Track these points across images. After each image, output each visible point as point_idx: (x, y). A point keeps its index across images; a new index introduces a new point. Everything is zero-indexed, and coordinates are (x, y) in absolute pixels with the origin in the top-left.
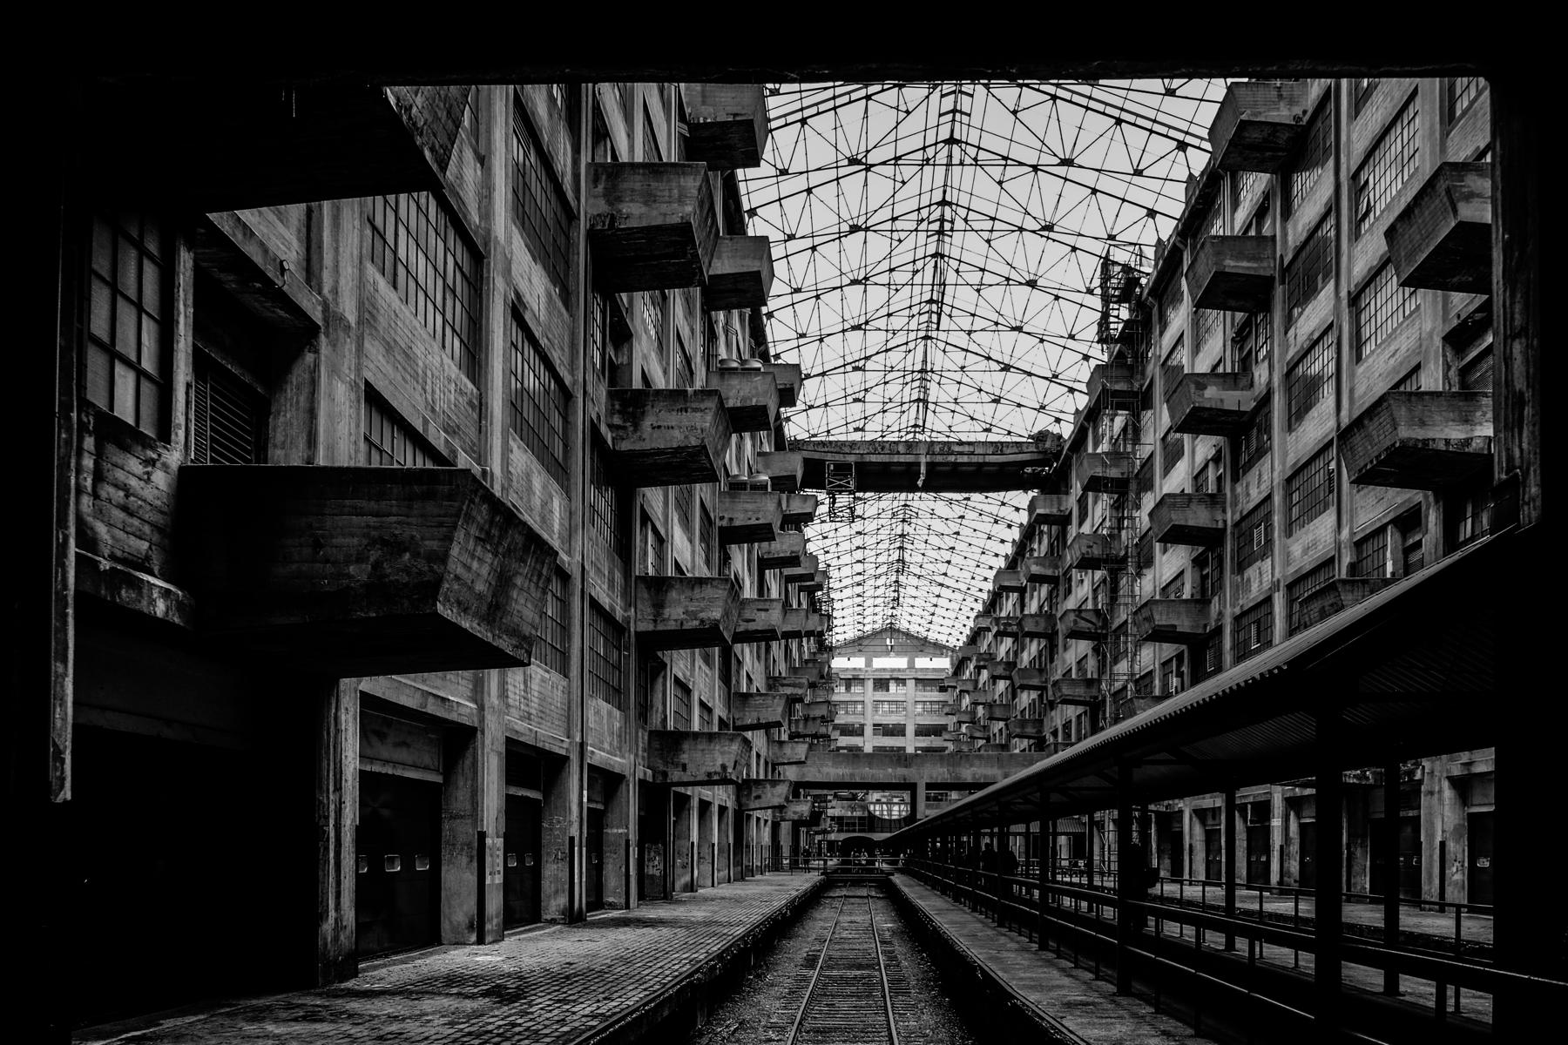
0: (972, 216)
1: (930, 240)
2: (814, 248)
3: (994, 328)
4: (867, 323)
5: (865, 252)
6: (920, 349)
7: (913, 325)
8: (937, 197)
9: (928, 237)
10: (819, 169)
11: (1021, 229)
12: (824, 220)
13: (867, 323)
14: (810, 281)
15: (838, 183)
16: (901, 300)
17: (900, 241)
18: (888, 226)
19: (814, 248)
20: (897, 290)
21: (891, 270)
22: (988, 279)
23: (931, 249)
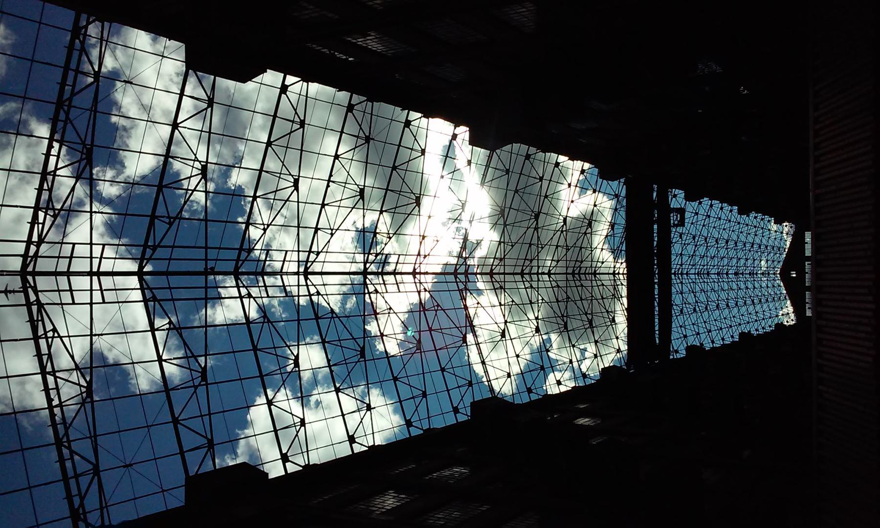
1: (541, 279)
4: (586, 314)
7: (589, 283)
9: (469, 281)
10: (507, 352)
15: (481, 343)
17: (543, 299)
20: (569, 298)
23: (546, 277)
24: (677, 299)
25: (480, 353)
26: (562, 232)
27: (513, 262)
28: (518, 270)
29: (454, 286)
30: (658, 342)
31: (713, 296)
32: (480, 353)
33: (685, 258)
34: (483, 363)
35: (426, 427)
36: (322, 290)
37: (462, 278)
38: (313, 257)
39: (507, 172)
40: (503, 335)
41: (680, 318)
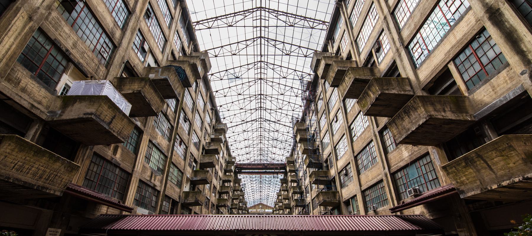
6: (260, 156)
8: (260, 117)
16: (255, 149)
22: (270, 139)
24: (254, 176)
25: (239, 125)
27: (264, 133)
28: (262, 135)
29: (257, 118)
30: (242, 171)
31: (255, 185)
32: (239, 125)
33: (265, 178)
34: (237, 125)
35: (220, 111)
36: (257, 83)
37: (260, 120)
38: (265, 81)
39: (288, 132)
40: (244, 131)
41: (249, 177)
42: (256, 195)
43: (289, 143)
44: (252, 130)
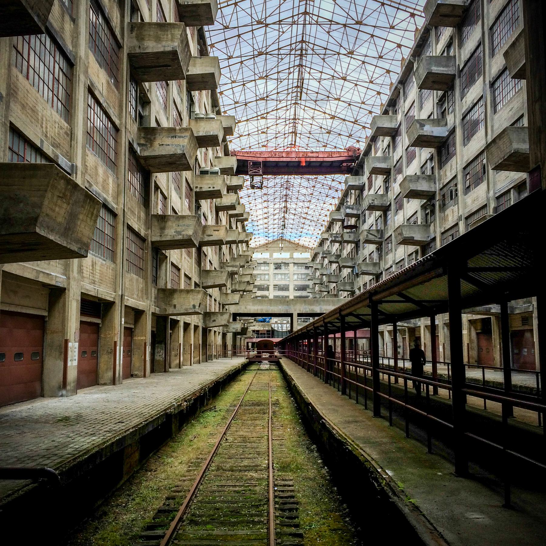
0: (316, 47)
1: (296, 59)
2: (242, 62)
3: (327, 99)
4: (267, 97)
5: (266, 64)
6: (293, 110)
7: (289, 98)
9: (295, 57)
11: (339, 54)
12: (247, 49)
13: (267, 97)
14: (240, 77)
17: (282, 59)
18: (276, 52)
19: (242, 62)
20: (281, 82)
21: (278, 72)
22: (324, 76)
23: (297, 63)
26: (328, 97)
42: (272, 217)
43: (378, 88)
44: (279, 49)
